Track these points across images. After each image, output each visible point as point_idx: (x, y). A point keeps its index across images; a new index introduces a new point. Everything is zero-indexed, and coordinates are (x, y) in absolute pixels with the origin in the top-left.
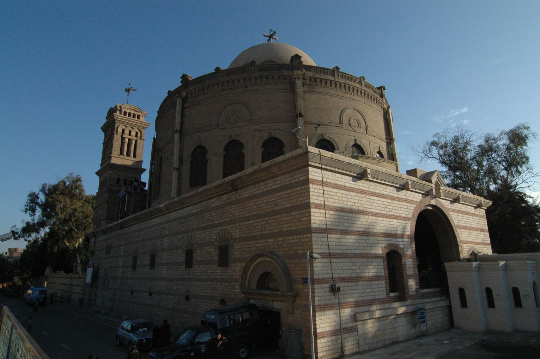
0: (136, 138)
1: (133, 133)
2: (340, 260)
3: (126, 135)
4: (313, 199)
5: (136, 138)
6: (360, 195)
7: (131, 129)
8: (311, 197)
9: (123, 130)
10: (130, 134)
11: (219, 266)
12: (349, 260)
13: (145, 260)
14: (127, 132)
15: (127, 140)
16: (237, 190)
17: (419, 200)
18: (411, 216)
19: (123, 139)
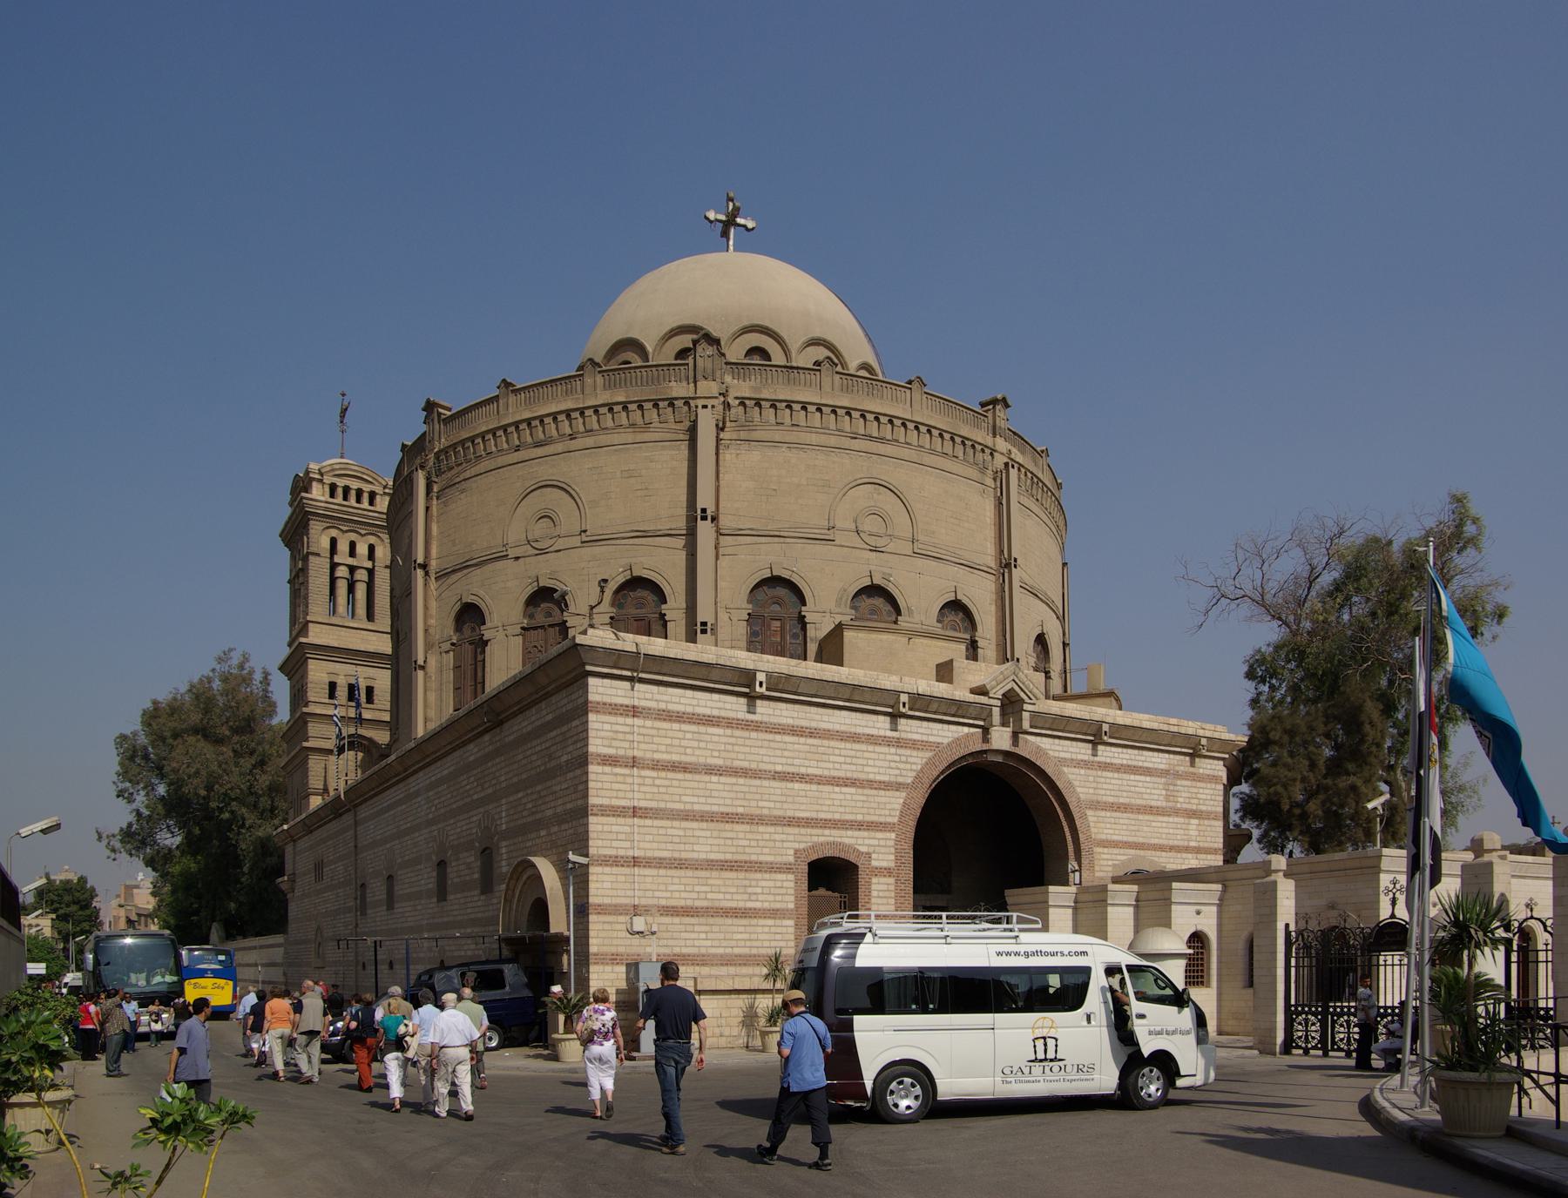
0: (369, 565)
1: (362, 549)
2: (662, 872)
3: (342, 557)
4: (596, 746)
5: (369, 565)
6: (738, 733)
7: (353, 537)
8: (591, 741)
9: (333, 542)
10: (352, 553)
11: (483, 893)
12: (690, 873)
13: (377, 891)
14: (343, 547)
15: (342, 572)
16: (501, 723)
17: (946, 741)
18: (909, 781)
19: (334, 566)
